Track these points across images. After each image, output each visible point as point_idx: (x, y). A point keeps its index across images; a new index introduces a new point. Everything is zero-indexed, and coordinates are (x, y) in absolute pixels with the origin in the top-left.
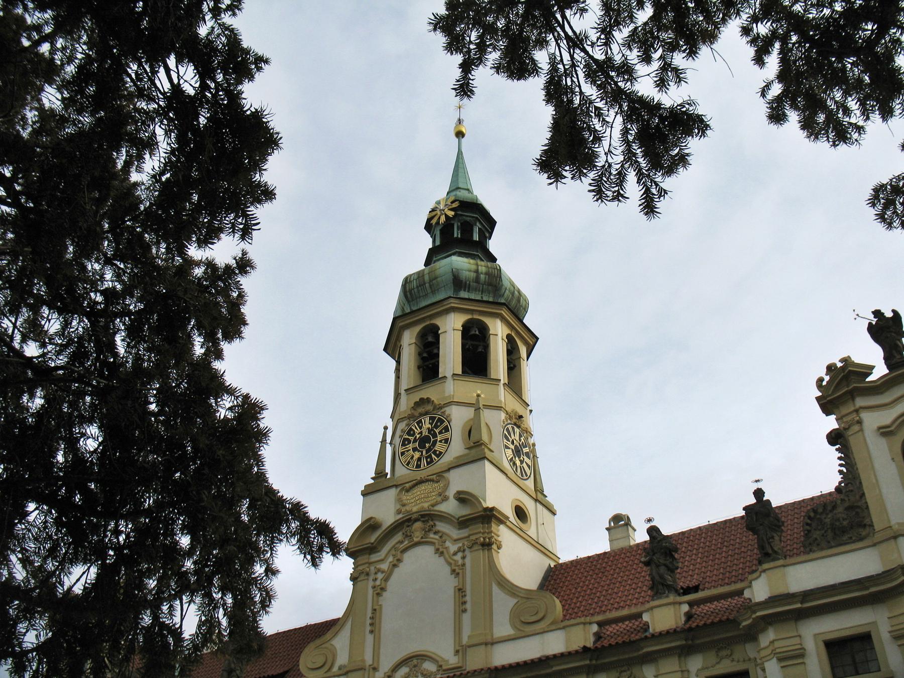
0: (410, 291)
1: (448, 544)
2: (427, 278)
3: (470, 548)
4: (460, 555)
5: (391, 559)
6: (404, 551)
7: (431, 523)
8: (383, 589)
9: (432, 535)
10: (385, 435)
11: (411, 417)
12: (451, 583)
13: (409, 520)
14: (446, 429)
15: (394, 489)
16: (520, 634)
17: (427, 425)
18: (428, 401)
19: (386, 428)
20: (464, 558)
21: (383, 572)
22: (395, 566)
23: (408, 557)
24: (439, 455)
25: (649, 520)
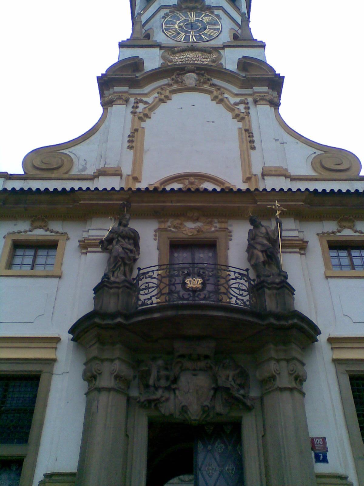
12: (235, 125)
22: (162, 101)
23: (175, 97)
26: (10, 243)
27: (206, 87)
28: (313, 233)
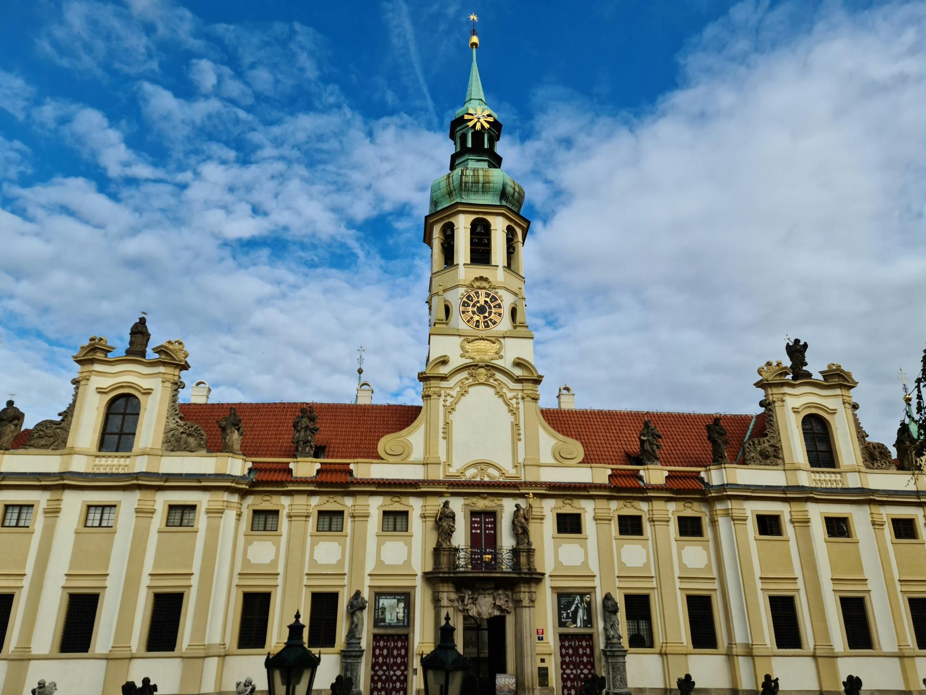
0: (466, 183)
5: (458, 389)
9: (491, 381)
12: (510, 418)
13: (476, 365)
15: (457, 337)
18: (486, 280)
20: (518, 403)
21: (452, 397)
23: (471, 390)
24: (494, 323)
27: (491, 381)
28: (549, 509)
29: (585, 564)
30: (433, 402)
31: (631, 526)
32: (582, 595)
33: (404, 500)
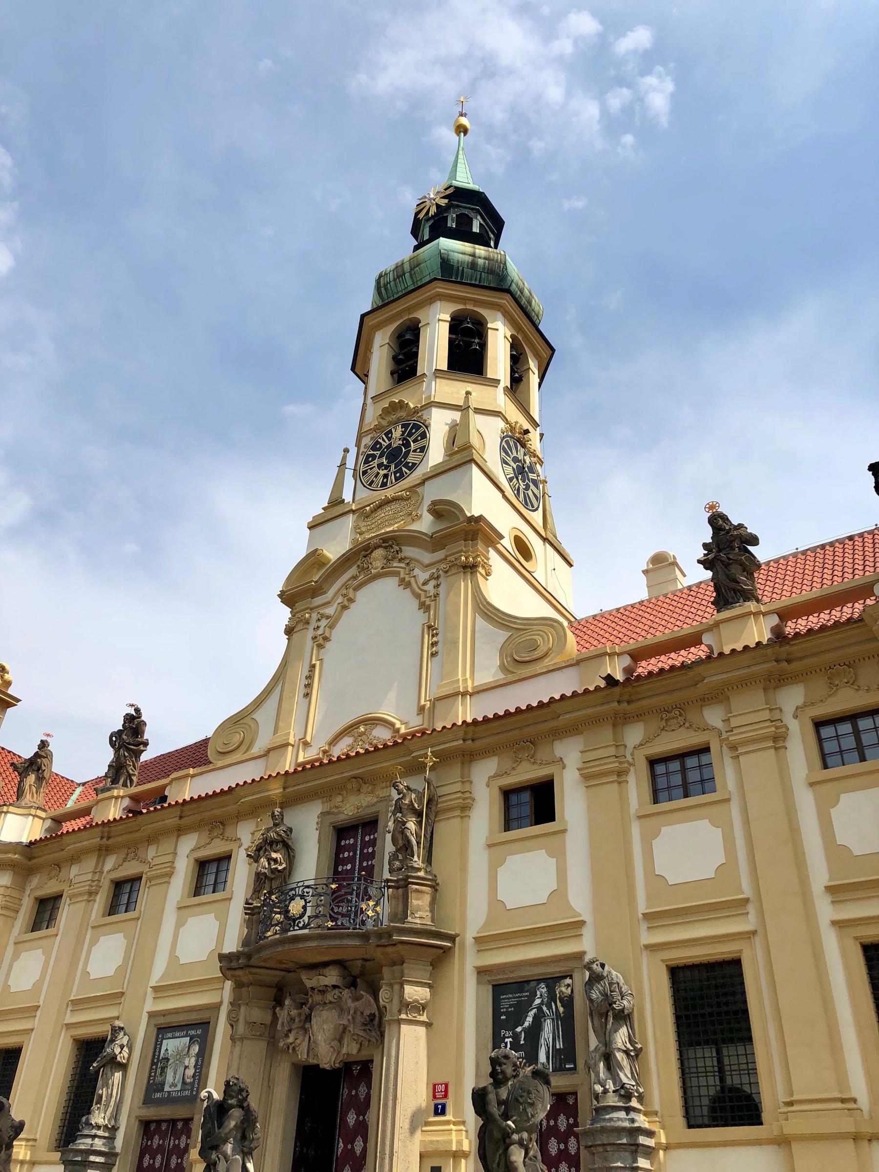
0: (385, 286)
1: (417, 571)
2: (407, 267)
3: (446, 572)
4: (433, 583)
6: (357, 588)
7: (396, 548)
8: (326, 639)
10: (344, 458)
11: (376, 429)
14: (424, 436)
16: (511, 677)
17: (397, 433)
19: (346, 451)
20: (437, 586)
22: (345, 608)
24: (413, 467)
25: (712, 507)
26: (192, 861)
29: (559, 894)
30: (295, 636)
31: (680, 776)
32: (552, 982)
33: (229, 833)
